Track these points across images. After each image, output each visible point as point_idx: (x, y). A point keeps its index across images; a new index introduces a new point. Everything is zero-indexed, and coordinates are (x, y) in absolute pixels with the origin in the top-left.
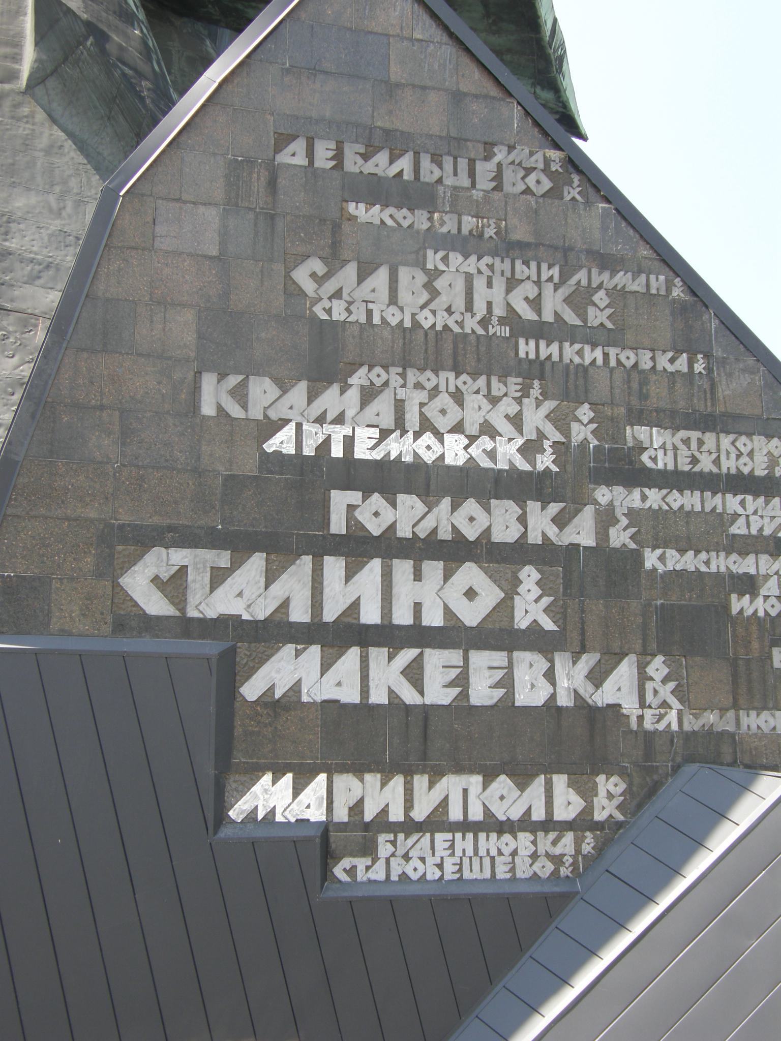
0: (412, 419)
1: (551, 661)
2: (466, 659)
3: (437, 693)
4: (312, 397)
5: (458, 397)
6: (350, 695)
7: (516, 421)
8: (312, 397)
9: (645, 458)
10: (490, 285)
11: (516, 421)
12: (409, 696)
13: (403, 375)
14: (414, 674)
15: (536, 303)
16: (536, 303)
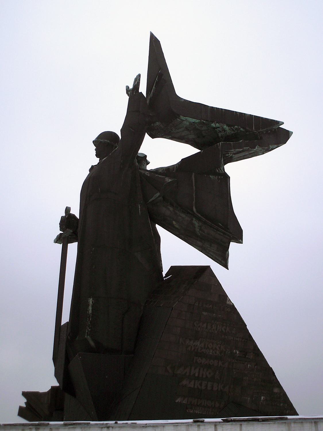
0: (206, 346)
1: (218, 384)
2: (208, 383)
3: (203, 387)
4: (194, 342)
5: (213, 344)
6: (192, 386)
7: (220, 348)
8: (194, 342)
9: (236, 355)
10: (220, 326)
11: (220, 348)
12: (200, 387)
13: (206, 339)
14: (201, 384)
15: (225, 330)
16: (225, 330)
